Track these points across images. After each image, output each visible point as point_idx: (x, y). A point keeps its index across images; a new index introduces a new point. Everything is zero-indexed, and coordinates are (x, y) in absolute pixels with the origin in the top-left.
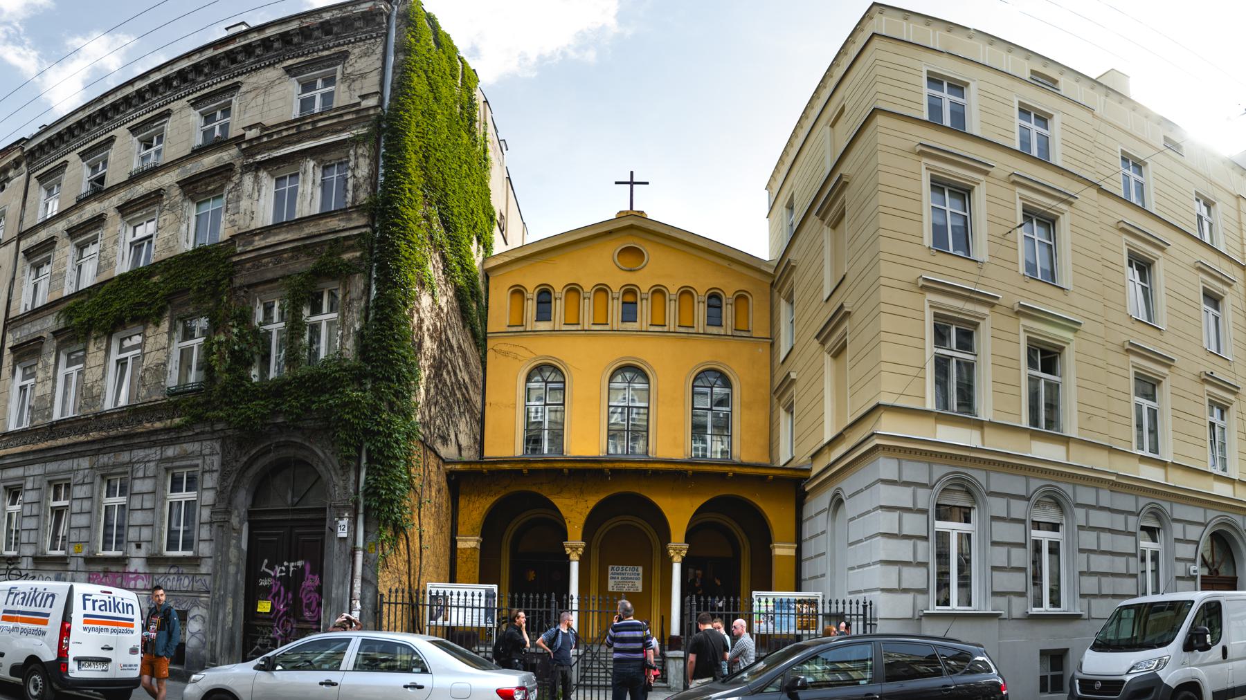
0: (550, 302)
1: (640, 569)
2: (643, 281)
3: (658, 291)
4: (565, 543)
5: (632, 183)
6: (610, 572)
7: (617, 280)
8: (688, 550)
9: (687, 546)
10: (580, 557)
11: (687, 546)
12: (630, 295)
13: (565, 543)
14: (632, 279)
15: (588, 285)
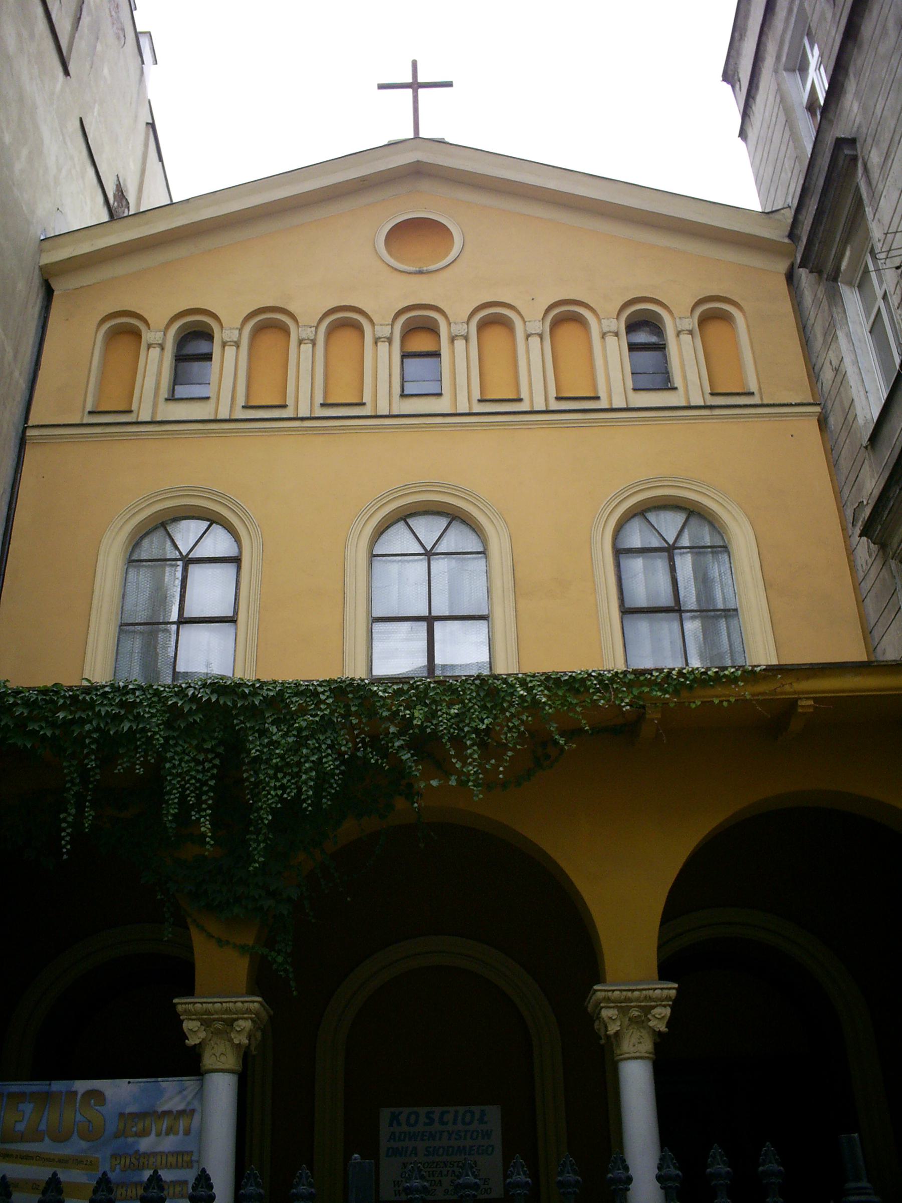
0: (208, 357)
1: (494, 1114)
2: (455, 294)
3: (494, 320)
4: (182, 1004)
5: (415, 86)
6: (385, 1130)
7: (385, 294)
8: (677, 1005)
9: (670, 989)
10: (246, 1056)
11: (670, 989)
12: (420, 330)
13: (182, 1004)
14: (423, 291)
15: (309, 305)
